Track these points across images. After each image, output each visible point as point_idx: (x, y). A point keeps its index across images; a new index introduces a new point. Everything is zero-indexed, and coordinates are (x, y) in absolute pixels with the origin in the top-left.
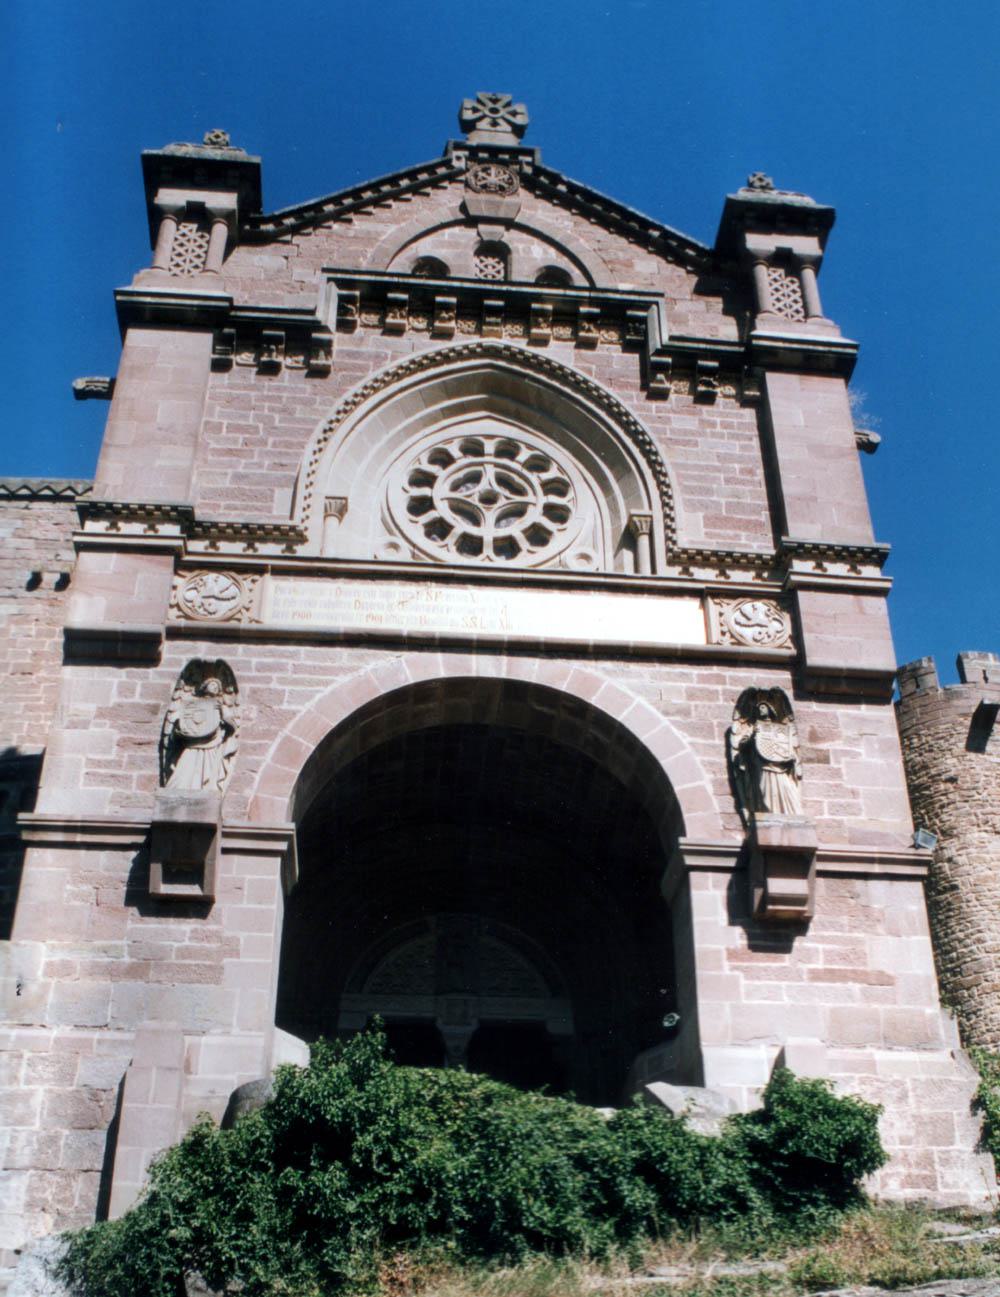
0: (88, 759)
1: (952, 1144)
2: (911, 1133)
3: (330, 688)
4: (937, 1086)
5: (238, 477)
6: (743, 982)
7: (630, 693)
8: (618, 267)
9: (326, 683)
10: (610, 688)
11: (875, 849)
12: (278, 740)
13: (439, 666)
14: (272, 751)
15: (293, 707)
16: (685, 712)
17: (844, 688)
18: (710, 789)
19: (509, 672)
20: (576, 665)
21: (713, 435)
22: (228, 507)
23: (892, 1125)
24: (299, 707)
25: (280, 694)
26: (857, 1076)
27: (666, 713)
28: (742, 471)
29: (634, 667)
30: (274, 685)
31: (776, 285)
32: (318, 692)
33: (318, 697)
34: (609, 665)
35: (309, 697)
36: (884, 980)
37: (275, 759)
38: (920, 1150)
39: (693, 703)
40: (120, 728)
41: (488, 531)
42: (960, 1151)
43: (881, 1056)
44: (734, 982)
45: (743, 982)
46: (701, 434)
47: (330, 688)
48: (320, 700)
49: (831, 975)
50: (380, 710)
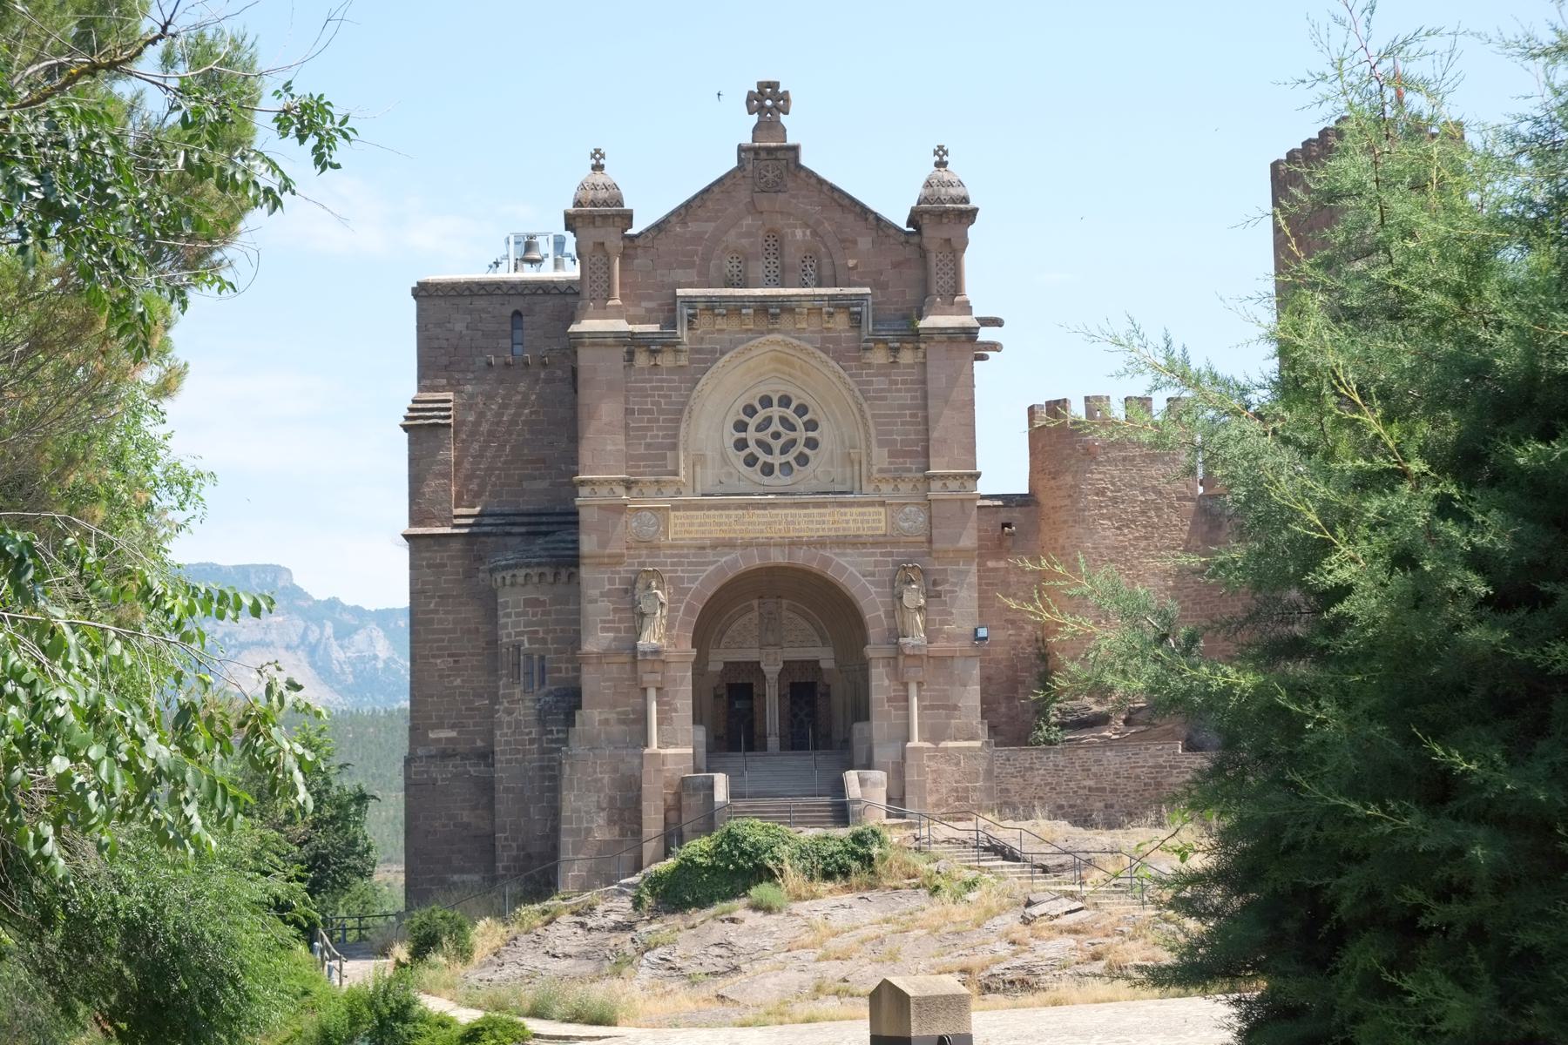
5: (648, 446)
10: (838, 563)
16: (873, 574)
22: (644, 466)
25: (683, 578)
27: (864, 576)
30: (679, 574)
31: (940, 265)
46: (889, 391)
49: (932, 707)
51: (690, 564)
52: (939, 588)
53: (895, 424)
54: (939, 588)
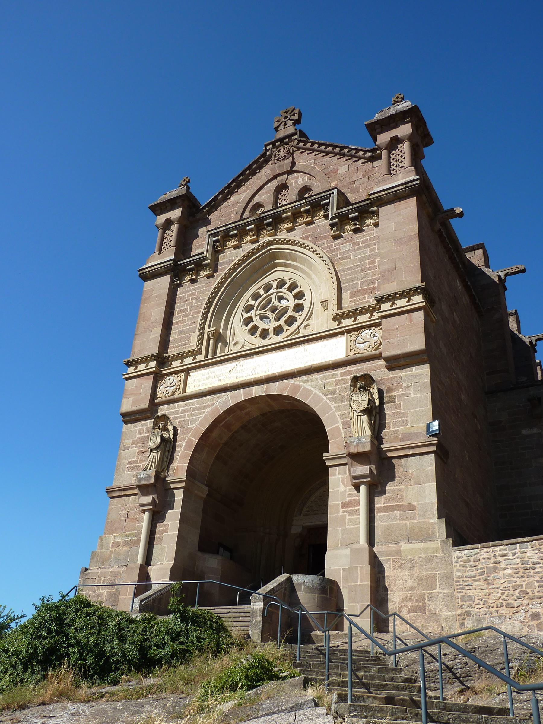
0: (129, 462)
1: (435, 589)
2: (415, 585)
3: (204, 415)
4: (429, 560)
6: (347, 517)
7: (312, 389)
8: (332, 174)
9: (202, 413)
10: (305, 388)
11: (409, 442)
12: (186, 441)
13: (241, 395)
14: (184, 445)
15: (192, 426)
16: (334, 392)
17: (402, 362)
18: (341, 427)
19: (266, 392)
20: (292, 381)
21: (358, 249)
23: (406, 581)
24: (194, 425)
25: (188, 421)
26: (392, 558)
27: (326, 395)
28: (369, 263)
29: (315, 376)
30: (187, 418)
32: (200, 417)
33: (200, 419)
34: (304, 378)
35: (197, 420)
36: (411, 508)
37: (184, 449)
38: (419, 593)
39: (337, 387)
40: (139, 447)
41: (271, 325)
42: (438, 592)
43: (404, 546)
44: (344, 518)
45: (347, 517)
47: (204, 415)
48: (201, 420)
50: (226, 418)
51: (194, 409)
52: (392, 394)
53: (356, 273)
54: (392, 394)
